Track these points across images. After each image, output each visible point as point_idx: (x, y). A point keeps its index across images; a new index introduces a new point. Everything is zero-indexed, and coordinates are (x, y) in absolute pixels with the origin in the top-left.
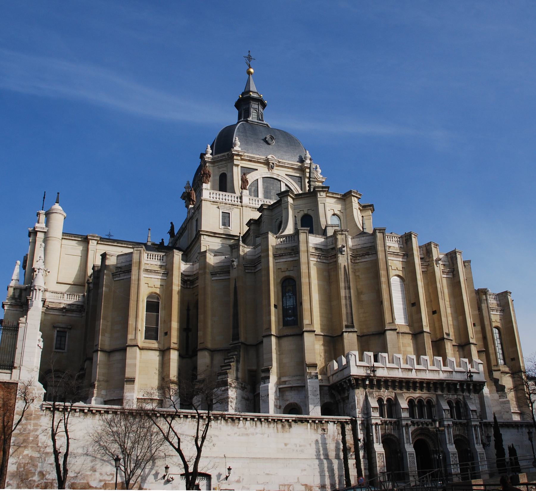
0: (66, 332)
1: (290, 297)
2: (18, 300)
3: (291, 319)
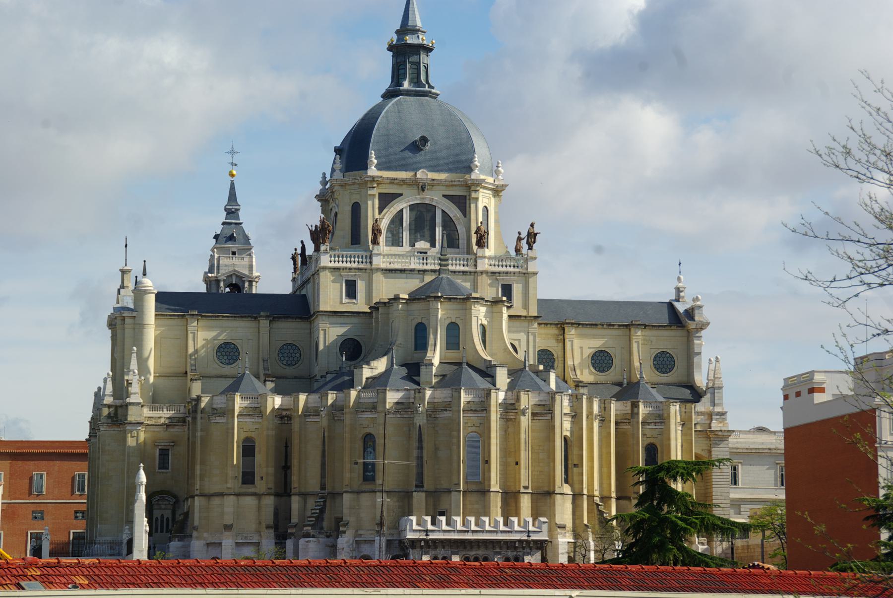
0: (169, 450)
1: (371, 453)
2: (114, 419)
3: (370, 474)
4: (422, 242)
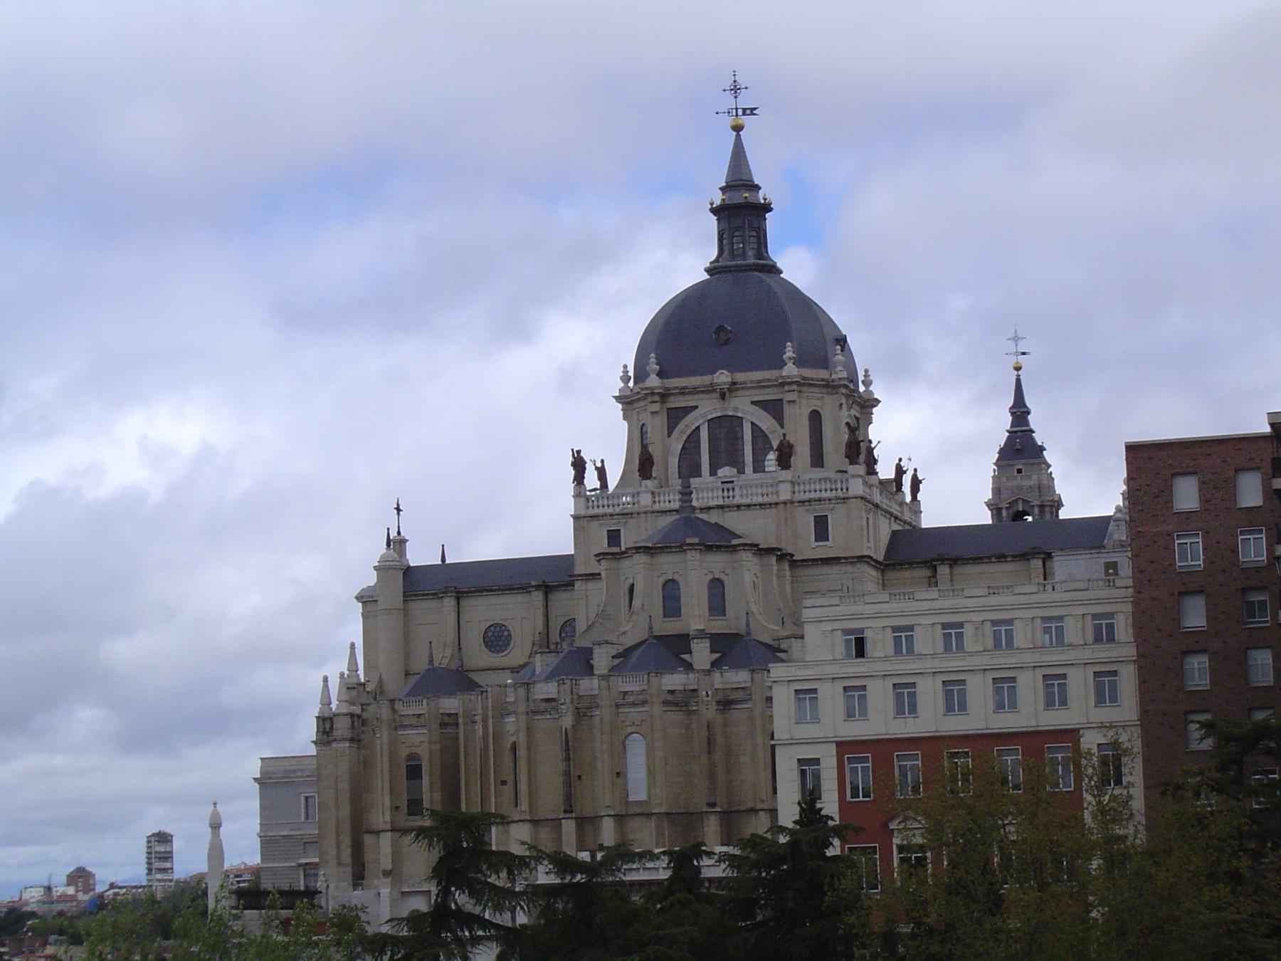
4: (727, 468)
